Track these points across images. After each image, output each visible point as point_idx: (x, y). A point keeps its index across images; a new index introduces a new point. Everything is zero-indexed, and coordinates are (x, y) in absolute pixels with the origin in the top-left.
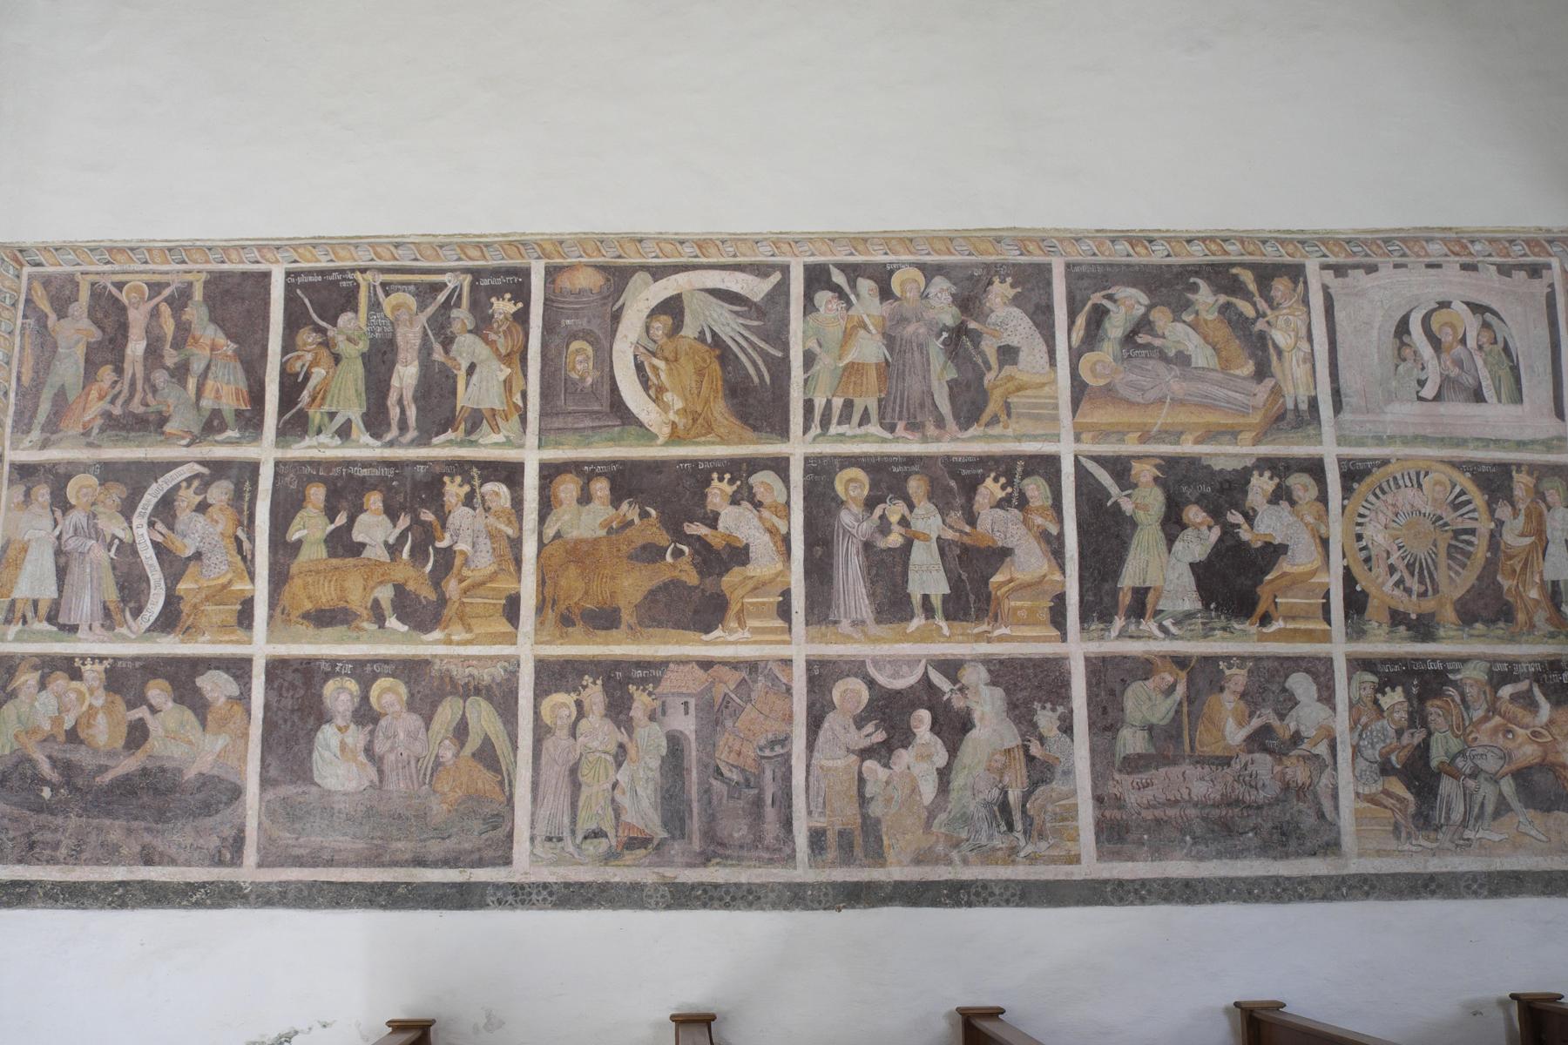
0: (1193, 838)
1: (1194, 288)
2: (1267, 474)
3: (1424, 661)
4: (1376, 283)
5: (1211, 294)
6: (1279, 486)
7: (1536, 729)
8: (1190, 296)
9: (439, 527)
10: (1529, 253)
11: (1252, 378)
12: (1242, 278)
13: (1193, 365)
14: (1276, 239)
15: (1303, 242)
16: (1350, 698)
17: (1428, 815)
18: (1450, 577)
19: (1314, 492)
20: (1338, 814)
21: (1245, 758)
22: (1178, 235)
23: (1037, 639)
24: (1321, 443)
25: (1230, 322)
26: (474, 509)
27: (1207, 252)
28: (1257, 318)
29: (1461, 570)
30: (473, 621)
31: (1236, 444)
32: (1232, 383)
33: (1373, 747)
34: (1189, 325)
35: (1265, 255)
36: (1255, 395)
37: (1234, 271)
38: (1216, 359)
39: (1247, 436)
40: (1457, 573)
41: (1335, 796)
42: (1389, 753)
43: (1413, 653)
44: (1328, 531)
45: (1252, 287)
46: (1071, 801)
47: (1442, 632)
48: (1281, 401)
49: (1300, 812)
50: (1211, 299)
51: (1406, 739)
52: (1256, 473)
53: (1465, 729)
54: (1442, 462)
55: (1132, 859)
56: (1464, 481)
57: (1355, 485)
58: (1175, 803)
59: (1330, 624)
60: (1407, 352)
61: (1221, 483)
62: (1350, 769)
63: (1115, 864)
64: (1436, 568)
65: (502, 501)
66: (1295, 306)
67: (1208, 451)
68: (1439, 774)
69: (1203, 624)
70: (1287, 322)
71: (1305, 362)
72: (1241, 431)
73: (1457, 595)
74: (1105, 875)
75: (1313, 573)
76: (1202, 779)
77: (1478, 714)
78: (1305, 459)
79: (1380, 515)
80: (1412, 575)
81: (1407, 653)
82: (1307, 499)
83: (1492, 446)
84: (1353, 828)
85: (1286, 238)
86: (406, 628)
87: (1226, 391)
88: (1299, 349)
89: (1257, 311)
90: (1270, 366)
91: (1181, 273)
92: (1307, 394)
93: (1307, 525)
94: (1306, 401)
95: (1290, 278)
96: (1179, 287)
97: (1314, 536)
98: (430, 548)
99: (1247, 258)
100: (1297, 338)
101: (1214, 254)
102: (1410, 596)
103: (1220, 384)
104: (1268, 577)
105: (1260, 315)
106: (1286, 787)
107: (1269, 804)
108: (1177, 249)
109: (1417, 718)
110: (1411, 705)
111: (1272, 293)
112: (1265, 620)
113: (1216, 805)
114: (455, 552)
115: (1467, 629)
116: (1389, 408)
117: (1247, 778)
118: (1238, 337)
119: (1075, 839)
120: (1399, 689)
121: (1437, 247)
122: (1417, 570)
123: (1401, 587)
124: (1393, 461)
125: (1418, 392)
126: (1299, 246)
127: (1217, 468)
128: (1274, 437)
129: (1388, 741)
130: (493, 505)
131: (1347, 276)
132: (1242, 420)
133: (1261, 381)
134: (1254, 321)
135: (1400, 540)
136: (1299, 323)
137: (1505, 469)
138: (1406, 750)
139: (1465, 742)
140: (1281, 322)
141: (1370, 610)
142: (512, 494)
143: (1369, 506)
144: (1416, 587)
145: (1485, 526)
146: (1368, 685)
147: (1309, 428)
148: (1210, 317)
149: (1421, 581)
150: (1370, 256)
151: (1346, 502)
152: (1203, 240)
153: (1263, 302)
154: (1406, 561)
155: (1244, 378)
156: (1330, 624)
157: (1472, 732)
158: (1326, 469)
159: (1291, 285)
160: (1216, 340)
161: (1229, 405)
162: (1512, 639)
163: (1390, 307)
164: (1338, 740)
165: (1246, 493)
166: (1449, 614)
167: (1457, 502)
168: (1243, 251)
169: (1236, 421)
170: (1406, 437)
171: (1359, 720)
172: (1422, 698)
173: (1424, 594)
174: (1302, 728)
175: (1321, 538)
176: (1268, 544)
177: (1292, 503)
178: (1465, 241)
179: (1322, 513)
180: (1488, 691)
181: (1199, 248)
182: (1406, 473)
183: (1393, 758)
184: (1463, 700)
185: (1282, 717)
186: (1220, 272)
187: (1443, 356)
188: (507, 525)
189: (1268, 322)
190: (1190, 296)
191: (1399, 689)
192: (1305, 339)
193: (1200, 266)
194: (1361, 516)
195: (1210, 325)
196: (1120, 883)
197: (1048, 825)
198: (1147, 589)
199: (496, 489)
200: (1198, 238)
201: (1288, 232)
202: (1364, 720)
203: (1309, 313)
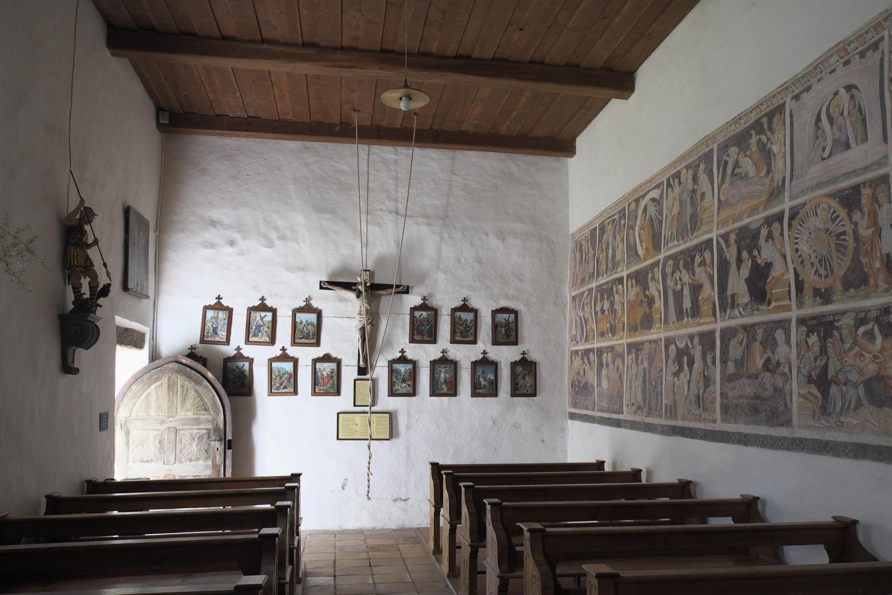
0: (745, 414)
3: (825, 316)
7: (875, 354)
16: (797, 341)
17: (825, 407)
18: (839, 263)
20: (792, 405)
21: (763, 374)
23: (707, 323)
29: (843, 258)
33: (805, 368)
40: (842, 260)
41: (791, 395)
42: (811, 371)
43: (822, 312)
44: (785, 250)
46: (715, 395)
47: (834, 298)
49: (778, 402)
51: (818, 363)
53: (842, 355)
55: (729, 423)
56: (835, 204)
58: (741, 397)
59: (791, 301)
62: (796, 380)
63: (726, 424)
64: (832, 259)
68: (831, 382)
69: (751, 308)
73: (842, 273)
74: (724, 429)
75: (783, 275)
76: (749, 385)
77: (847, 346)
79: (804, 236)
80: (821, 265)
81: (820, 312)
84: (797, 412)
93: (778, 249)
97: (781, 255)
102: (821, 279)
104: (768, 280)
106: (775, 389)
107: (770, 398)
109: (824, 351)
110: (821, 342)
112: (769, 304)
113: (752, 399)
115: (846, 294)
117: (763, 385)
119: (715, 412)
120: (815, 334)
122: (823, 263)
123: (817, 274)
129: (811, 364)
135: (814, 248)
137: (857, 188)
138: (818, 368)
139: (842, 363)
141: (805, 290)
143: (799, 232)
144: (823, 273)
145: (849, 228)
146: (804, 333)
149: (826, 269)
151: (790, 232)
154: (818, 259)
156: (791, 301)
157: (844, 357)
162: (867, 297)
164: (792, 364)
166: (839, 286)
171: (801, 352)
172: (825, 339)
173: (826, 277)
174: (780, 359)
175: (783, 255)
176: (766, 263)
177: (773, 239)
179: (782, 241)
180: (853, 331)
183: (813, 374)
184: (841, 338)
185: (773, 353)
191: (815, 334)
194: (796, 238)
196: (728, 433)
197: (709, 405)
198: (735, 294)
202: (802, 352)
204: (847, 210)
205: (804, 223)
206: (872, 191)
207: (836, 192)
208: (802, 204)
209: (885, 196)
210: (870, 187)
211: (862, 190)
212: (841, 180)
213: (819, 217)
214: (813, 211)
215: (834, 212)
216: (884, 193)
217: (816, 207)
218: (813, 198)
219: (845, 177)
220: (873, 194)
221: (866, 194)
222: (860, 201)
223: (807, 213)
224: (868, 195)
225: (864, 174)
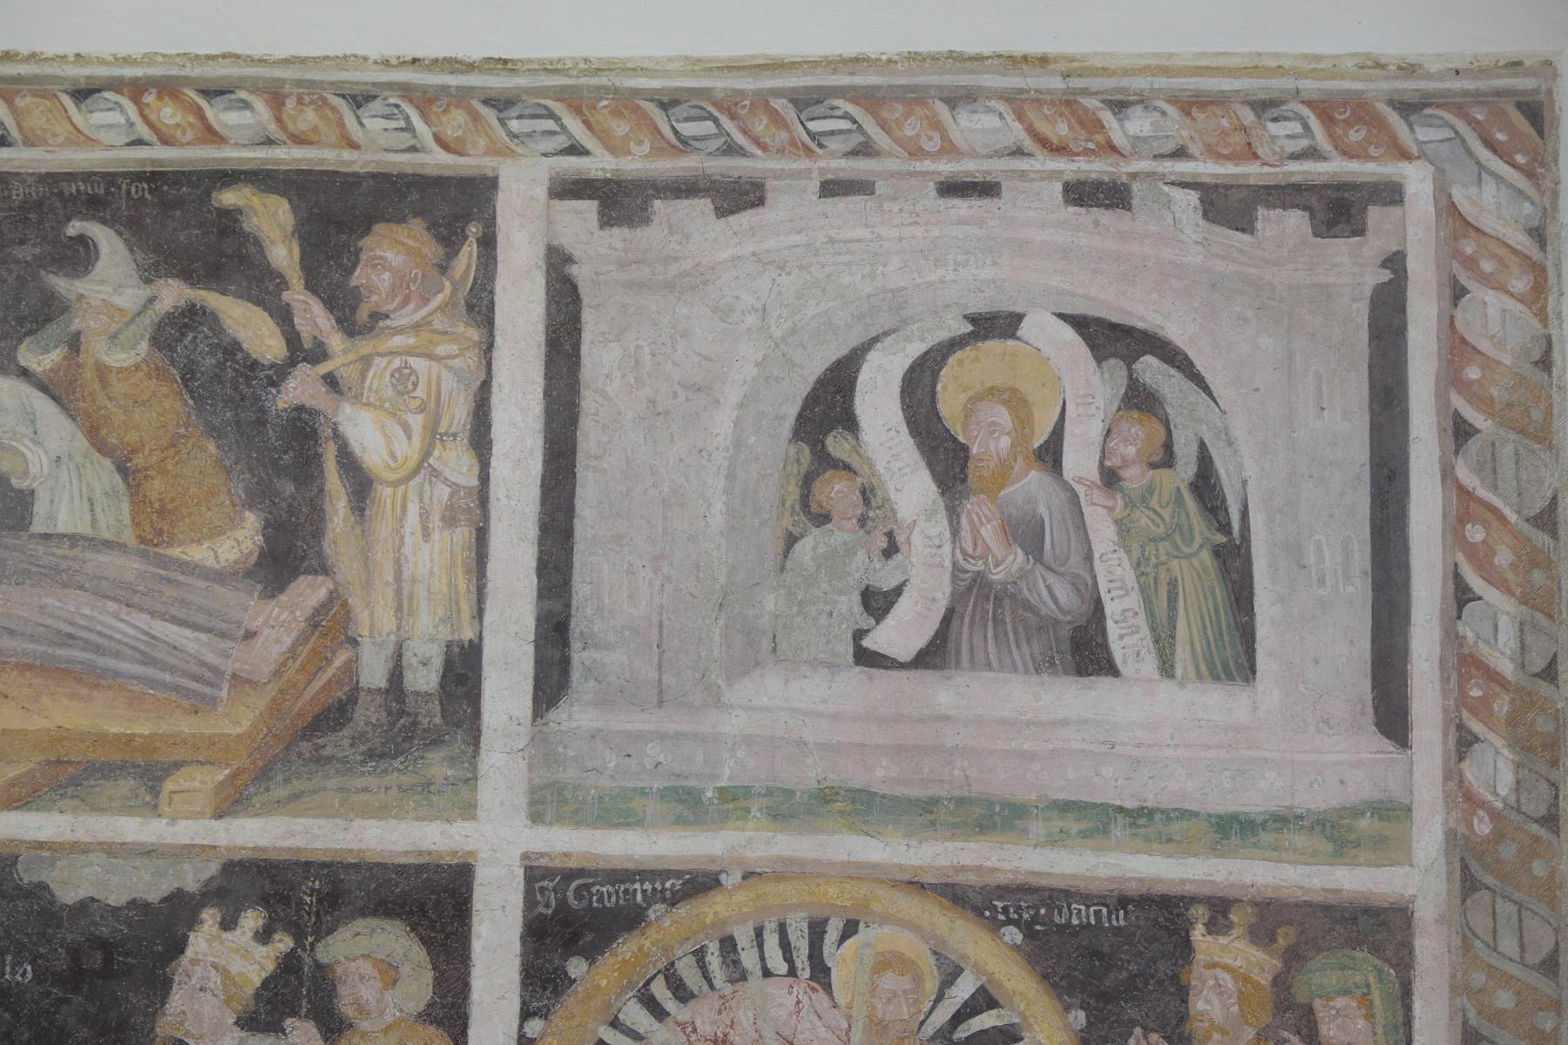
1: (79, 256)
2: (252, 920)
4: (750, 248)
5: (135, 279)
6: (288, 966)
8: (60, 284)
10: (1324, 144)
11: (249, 574)
12: (251, 223)
13: (38, 527)
14: (405, 90)
15: (502, 103)
19: (418, 987)
22: (49, 70)
24: (469, 810)
25: (188, 375)
27: (144, 131)
28: (292, 362)
31: (154, 809)
32: (169, 591)
34: (43, 387)
35: (353, 146)
36: (250, 635)
37: (229, 198)
38: (126, 507)
39: (199, 781)
45: (283, 254)
48: (341, 659)
50: (130, 296)
52: (210, 916)
54: (916, 886)
57: (576, 967)
60: (836, 492)
61: (75, 953)
66: (439, 322)
67: (43, 836)
70: (404, 380)
71: (450, 521)
72: (178, 765)
78: (402, 869)
82: (391, 1015)
83: (1118, 831)
85: (444, 88)
87: (143, 620)
88: (435, 474)
89: (292, 339)
90: (318, 534)
91: (39, 204)
92: (445, 634)
94: (438, 663)
95: (432, 226)
96: (26, 252)
99: (287, 156)
100: (434, 434)
101: (166, 141)
103: (126, 596)
105: (301, 352)
108: (36, 121)
111: (358, 277)
116: (745, 690)
118: (215, 432)
121: (990, 121)
124: (731, 880)
125: (859, 635)
126: (489, 114)
127: (68, 896)
128: (297, 785)
131: (646, 221)
132: (186, 726)
133: (281, 589)
134: (277, 376)
136: (448, 382)
140: (380, 376)
147: (435, 755)
148: (119, 359)
150: (738, 151)
152: (136, 89)
153: (317, 308)
155: (219, 577)
158: (478, 903)
159: (432, 250)
160: (132, 437)
161: (150, 671)
163: (793, 331)
165: (163, 987)
167: (961, 1033)
168: (272, 128)
169: (164, 728)
170: (789, 793)
178: (1091, 103)
181: (115, 117)
182: (770, 928)
186: (179, 203)
187: (975, 508)
189: (331, 381)
190: (60, 284)
192: (463, 441)
193: (110, 179)
195: (118, 388)
200: (116, 85)
201: (453, 65)
203: (488, 348)
204: (1079, 1018)
205: (682, 993)
206: (1278, 964)
207: (1004, 891)
208: (678, 874)
209: (1370, 1017)
210: (1262, 934)
211: (1198, 934)
212: (1037, 828)
213: (841, 1000)
214: (785, 945)
215: (984, 1000)
216: (1365, 1001)
217: (817, 930)
218: (785, 871)
219: (1075, 828)
220: (1280, 982)
221: (1226, 968)
222: (1183, 994)
223: (728, 945)
224: (1246, 979)
225: (1215, 850)
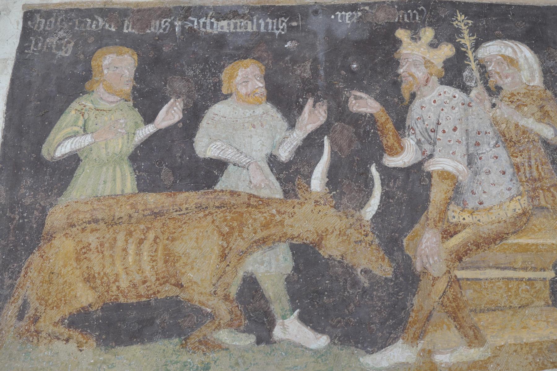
9: (390, 126)
26: (466, 89)
30: (483, 320)
65: (525, 75)
86: (323, 341)
98: (373, 170)
114: (430, 175)
130: (507, 84)
142: (542, 62)
188: (540, 121)
199: (509, 52)
